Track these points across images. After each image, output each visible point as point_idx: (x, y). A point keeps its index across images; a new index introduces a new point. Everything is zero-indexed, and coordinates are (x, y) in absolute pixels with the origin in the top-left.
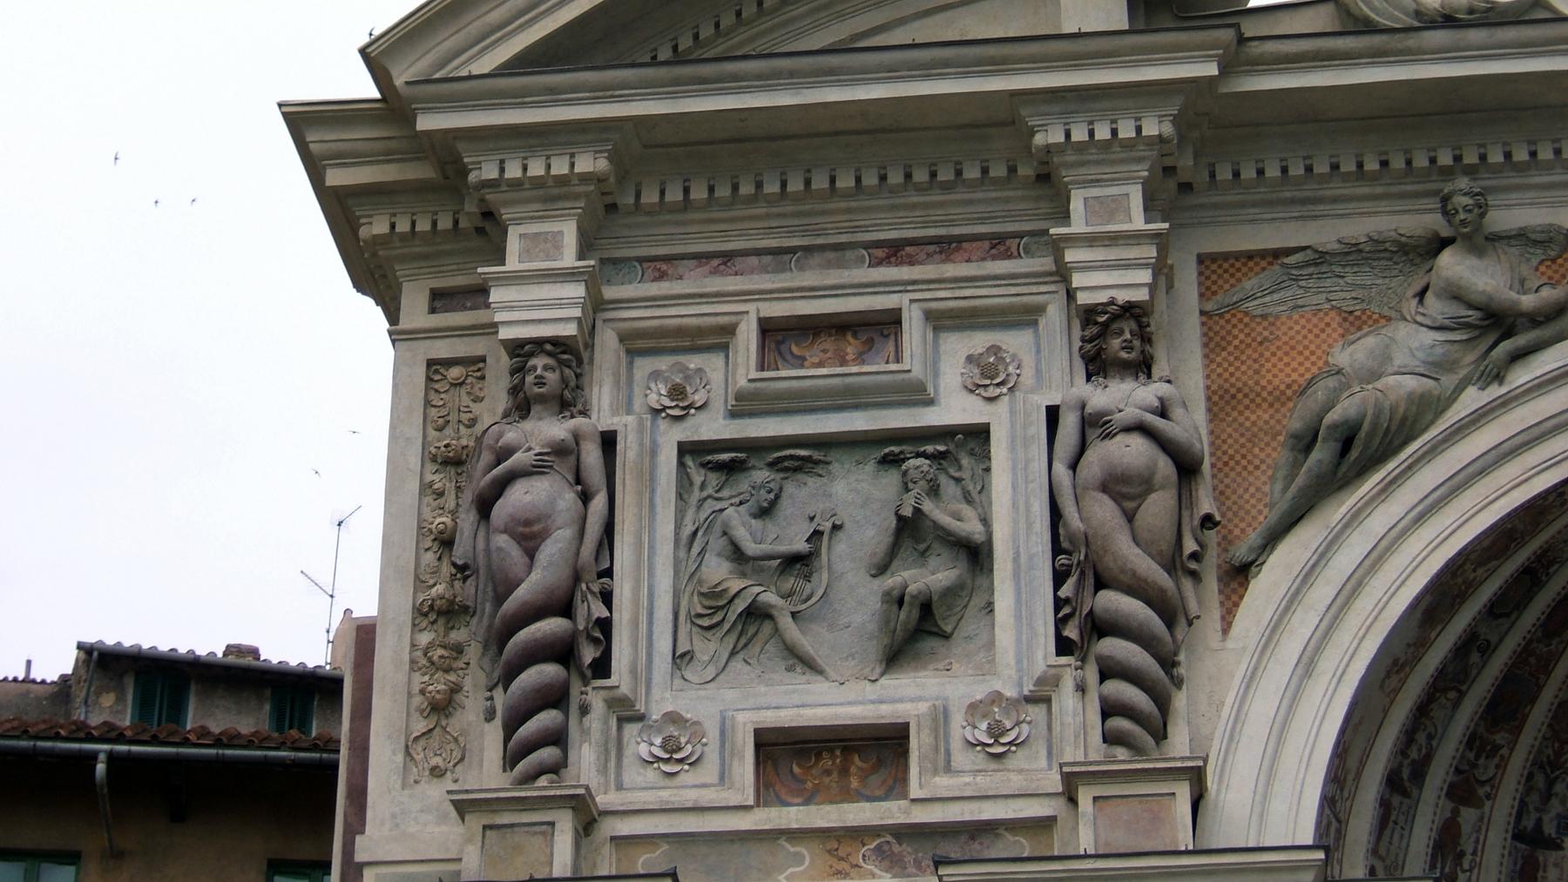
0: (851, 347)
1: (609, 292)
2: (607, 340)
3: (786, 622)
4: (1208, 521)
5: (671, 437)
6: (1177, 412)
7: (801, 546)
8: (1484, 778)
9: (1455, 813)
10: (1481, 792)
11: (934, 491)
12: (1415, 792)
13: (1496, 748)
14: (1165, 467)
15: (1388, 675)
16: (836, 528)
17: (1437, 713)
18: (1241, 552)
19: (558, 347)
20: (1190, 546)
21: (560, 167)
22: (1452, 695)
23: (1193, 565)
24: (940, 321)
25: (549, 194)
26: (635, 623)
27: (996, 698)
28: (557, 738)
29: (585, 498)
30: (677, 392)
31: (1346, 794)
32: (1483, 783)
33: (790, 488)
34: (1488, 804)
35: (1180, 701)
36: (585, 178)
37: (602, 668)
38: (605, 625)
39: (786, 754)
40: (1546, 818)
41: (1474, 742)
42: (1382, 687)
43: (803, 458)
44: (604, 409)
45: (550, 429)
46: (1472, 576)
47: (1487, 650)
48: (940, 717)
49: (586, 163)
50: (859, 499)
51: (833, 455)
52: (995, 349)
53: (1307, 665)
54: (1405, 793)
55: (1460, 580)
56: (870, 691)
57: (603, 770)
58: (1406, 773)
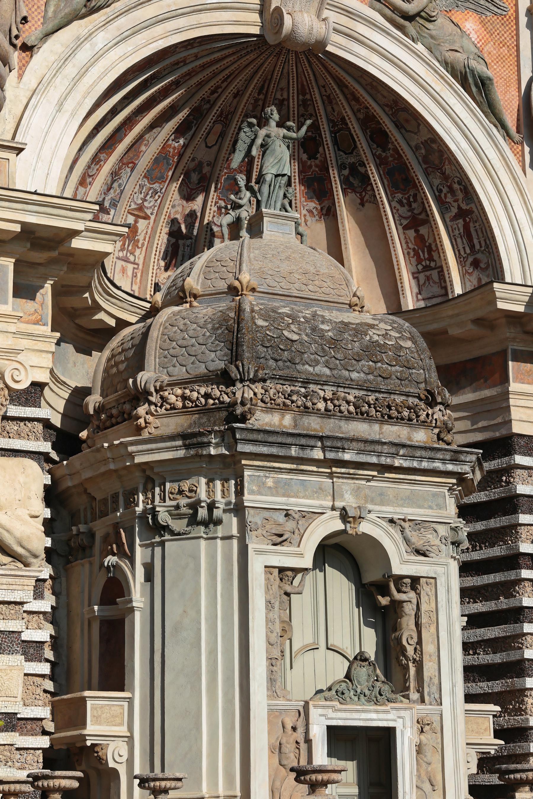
8: (91, 174)
32: (90, 176)
34: (89, 186)
40: (107, 198)
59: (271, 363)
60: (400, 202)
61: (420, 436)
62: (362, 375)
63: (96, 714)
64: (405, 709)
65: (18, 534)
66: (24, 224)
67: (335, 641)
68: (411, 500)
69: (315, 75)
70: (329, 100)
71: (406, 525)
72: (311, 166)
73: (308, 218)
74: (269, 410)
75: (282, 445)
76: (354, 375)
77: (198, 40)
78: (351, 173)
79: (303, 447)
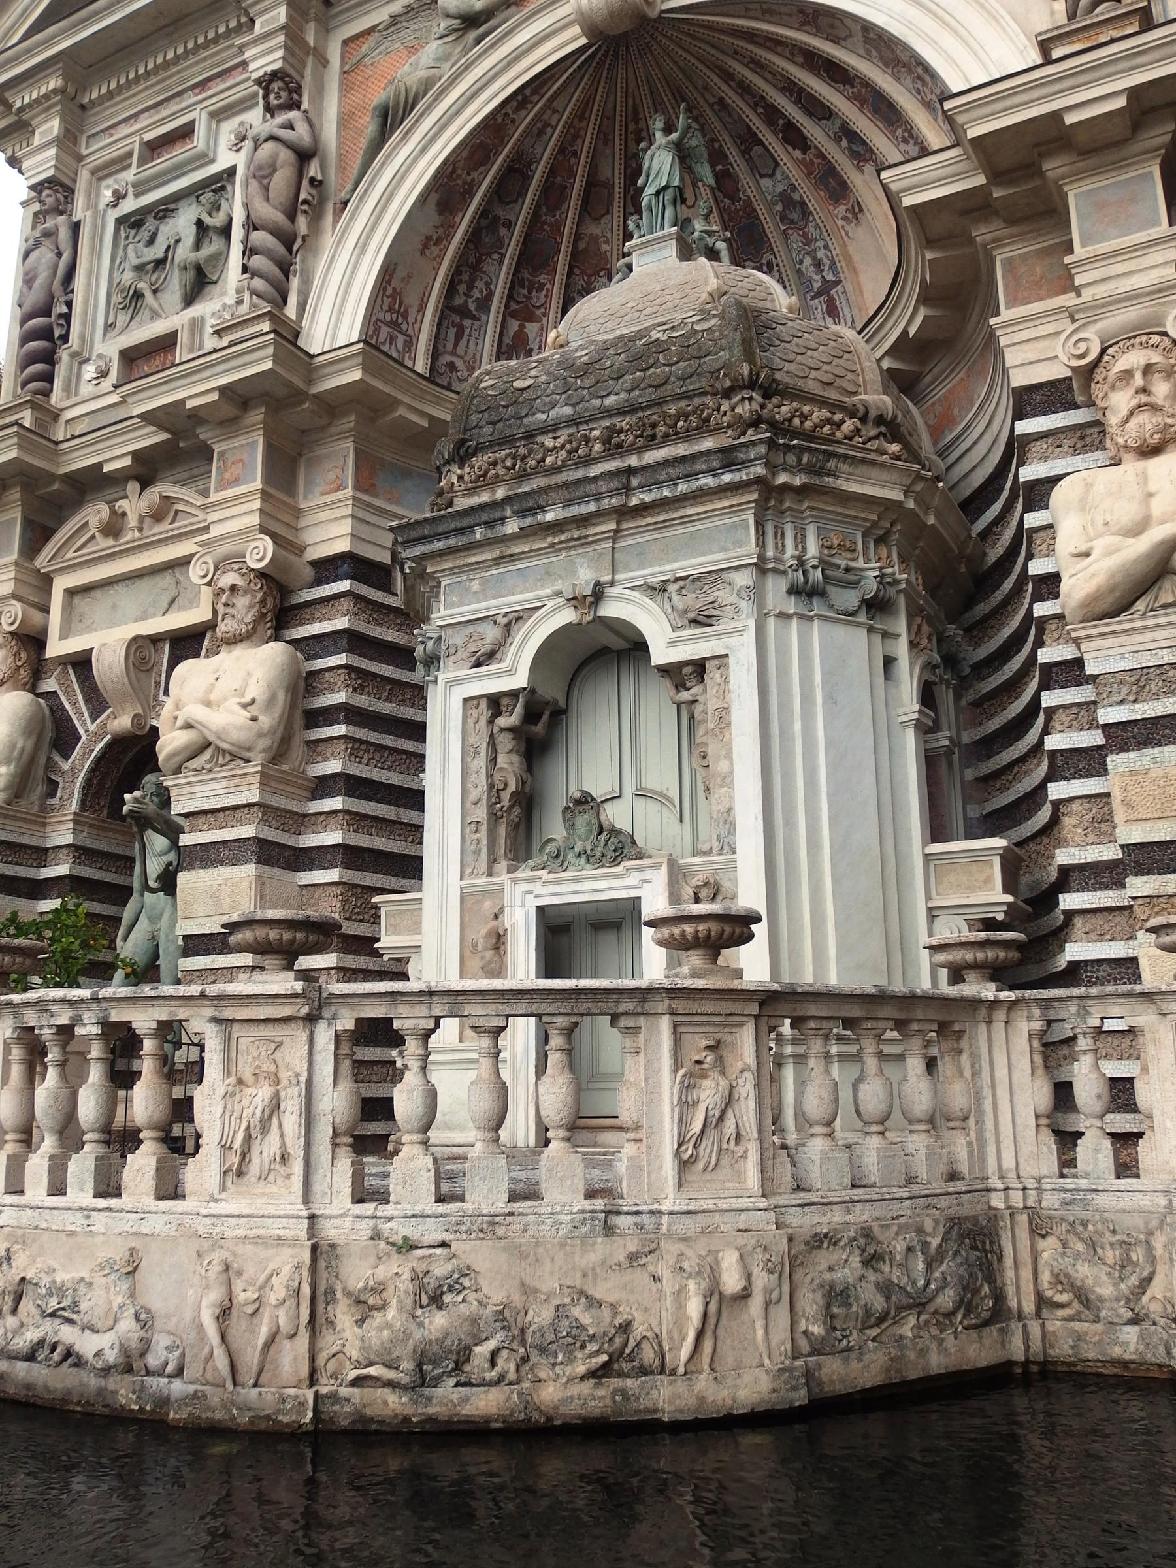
1: (84, 152)
2: (84, 176)
3: (148, 294)
4: (312, 180)
7: (160, 255)
9: (522, 327)
10: (539, 312)
12: (484, 317)
13: (541, 286)
14: (285, 155)
15: (425, 246)
16: (178, 241)
17: (488, 267)
18: (343, 195)
21: (43, 91)
22: (495, 256)
23: (305, 207)
24: (219, 116)
26: (85, 313)
27: (225, 306)
28: (49, 378)
29: (59, 255)
31: (411, 319)
33: (162, 228)
34: (545, 319)
36: (55, 91)
37: (65, 338)
38: (67, 317)
41: (516, 282)
42: (422, 253)
43: (164, 210)
44: (80, 210)
46: (469, 179)
47: (510, 225)
49: (52, 85)
50: (183, 222)
51: (182, 204)
52: (242, 123)
53: (362, 247)
54: (474, 318)
55: (459, 182)
57: (67, 389)
58: (472, 307)
59: (488, 429)
60: (905, 141)
62: (623, 395)
63: (392, 921)
64: (652, 867)
65: (214, 728)
67: (651, 781)
68: (692, 546)
69: (713, 46)
70: (759, 66)
71: (672, 588)
72: (812, 161)
73: (847, 228)
75: (460, 531)
76: (610, 401)
77: (528, 92)
78: (850, 142)
79: (490, 524)
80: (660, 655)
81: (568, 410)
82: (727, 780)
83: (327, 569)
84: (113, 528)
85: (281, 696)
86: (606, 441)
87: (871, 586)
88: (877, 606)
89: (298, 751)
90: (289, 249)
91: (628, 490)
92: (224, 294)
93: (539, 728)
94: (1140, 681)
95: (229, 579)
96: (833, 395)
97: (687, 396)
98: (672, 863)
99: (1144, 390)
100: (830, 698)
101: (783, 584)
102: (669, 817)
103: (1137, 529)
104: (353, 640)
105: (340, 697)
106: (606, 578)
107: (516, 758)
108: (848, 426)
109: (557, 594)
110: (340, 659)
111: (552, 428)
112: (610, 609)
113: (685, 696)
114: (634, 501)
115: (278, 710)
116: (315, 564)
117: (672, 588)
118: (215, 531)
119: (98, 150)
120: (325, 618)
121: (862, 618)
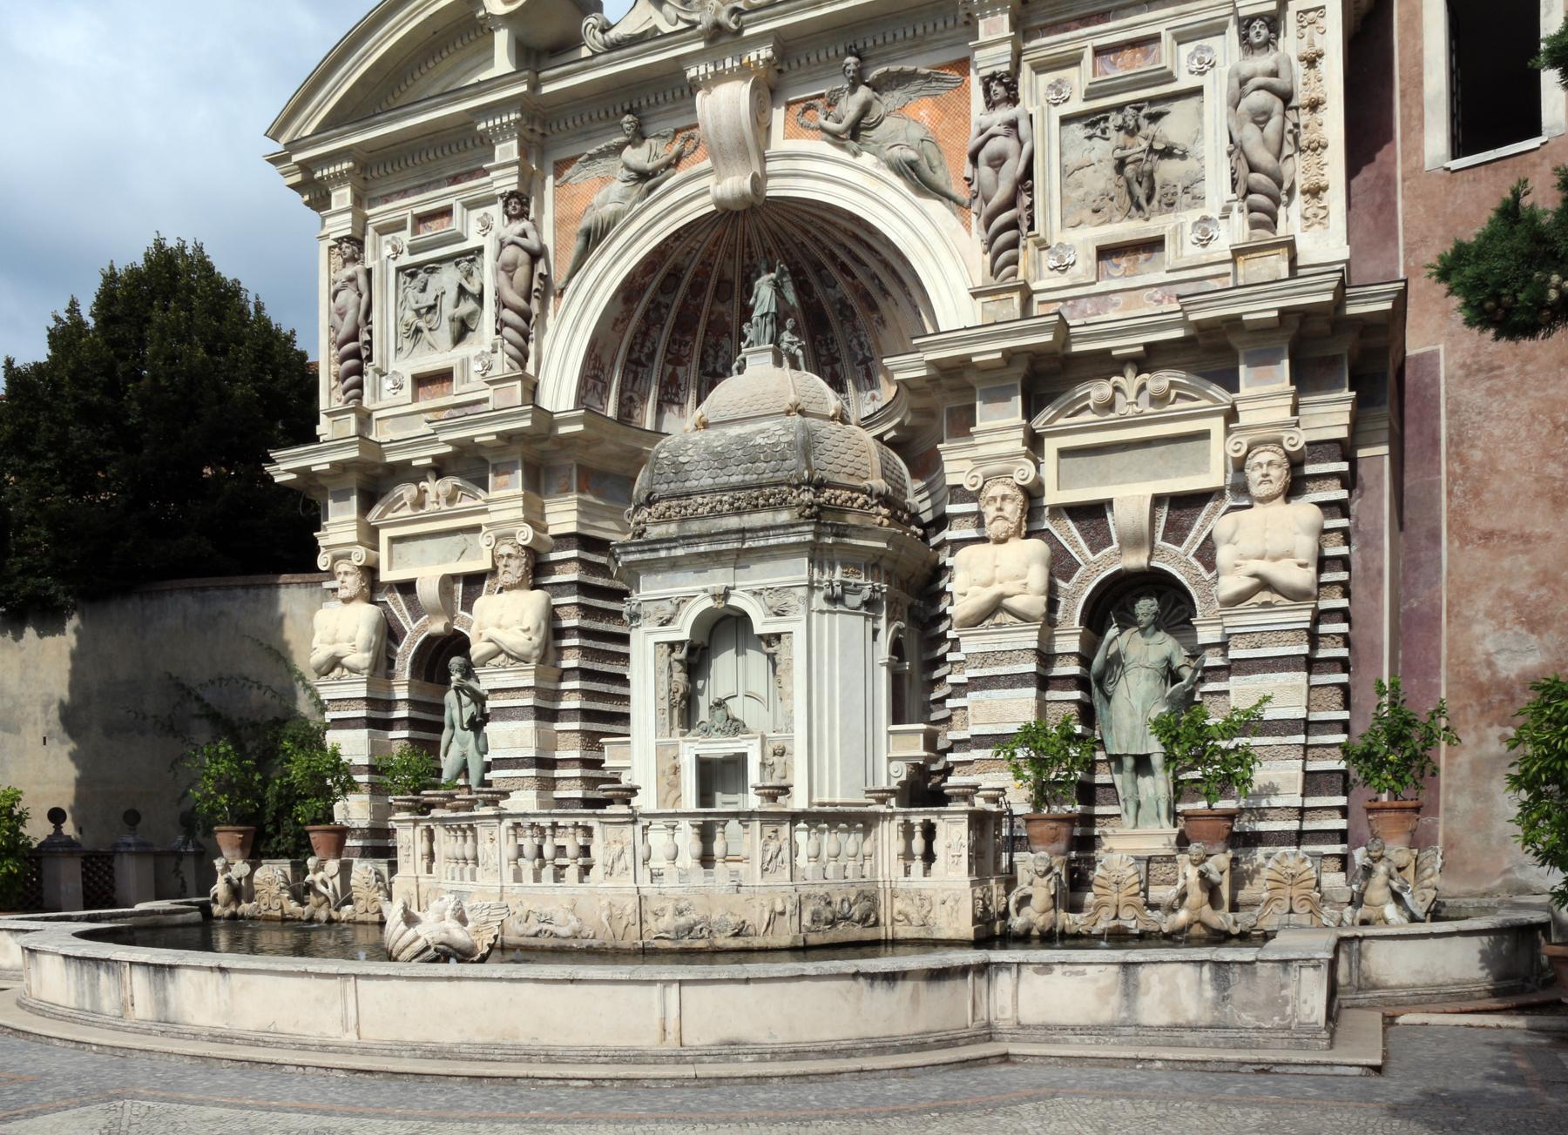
0: (445, 220)
3: (426, 331)
5: (393, 265)
6: (532, 234)
7: (432, 302)
11: (470, 273)
19: (349, 239)
20: (535, 286)
24: (470, 206)
25: (339, 179)
29: (360, 295)
30: (394, 248)
35: (532, 347)
38: (370, 343)
39: (422, 381)
45: (350, 270)
48: (465, 363)
50: (449, 278)
56: (448, 355)
61: (784, 517)
66: (497, 434)
74: (656, 524)
76: (734, 479)
80: (759, 629)
81: (710, 481)
82: (790, 696)
83: (563, 540)
84: (419, 503)
85: (543, 625)
86: (732, 504)
87: (867, 593)
88: (870, 604)
89: (552, 655)
90: (528, 322)
91: (743, 541)
92: (481, 342)
93: (695, 659)
94: (985, 658)
95: (505, 549)
96: (854, 482)
97: (776, 484)
98: (763, 738)
99: (1000, 509)
100: (843, 655)
101: (822, 594)
102: (763, 709)
103: (988, 584)
104: (583, 588)
105: (574, 622)
106: (731, 584)
107: (683, 675)
108: (860, 501)
109: (705, 591)
110: (574, 599)
111: (702, 493)
112: (732, 601)
113: (771, 650)
114: (746, 546)
115: (542, 633)
116: (554, 537)
117: (765, 593)
118: (494, 518)
119: (379, 213)
120: (562, 572)
121: (863, 610)
